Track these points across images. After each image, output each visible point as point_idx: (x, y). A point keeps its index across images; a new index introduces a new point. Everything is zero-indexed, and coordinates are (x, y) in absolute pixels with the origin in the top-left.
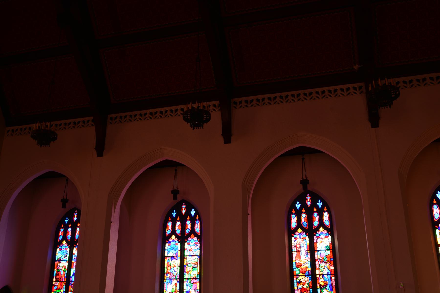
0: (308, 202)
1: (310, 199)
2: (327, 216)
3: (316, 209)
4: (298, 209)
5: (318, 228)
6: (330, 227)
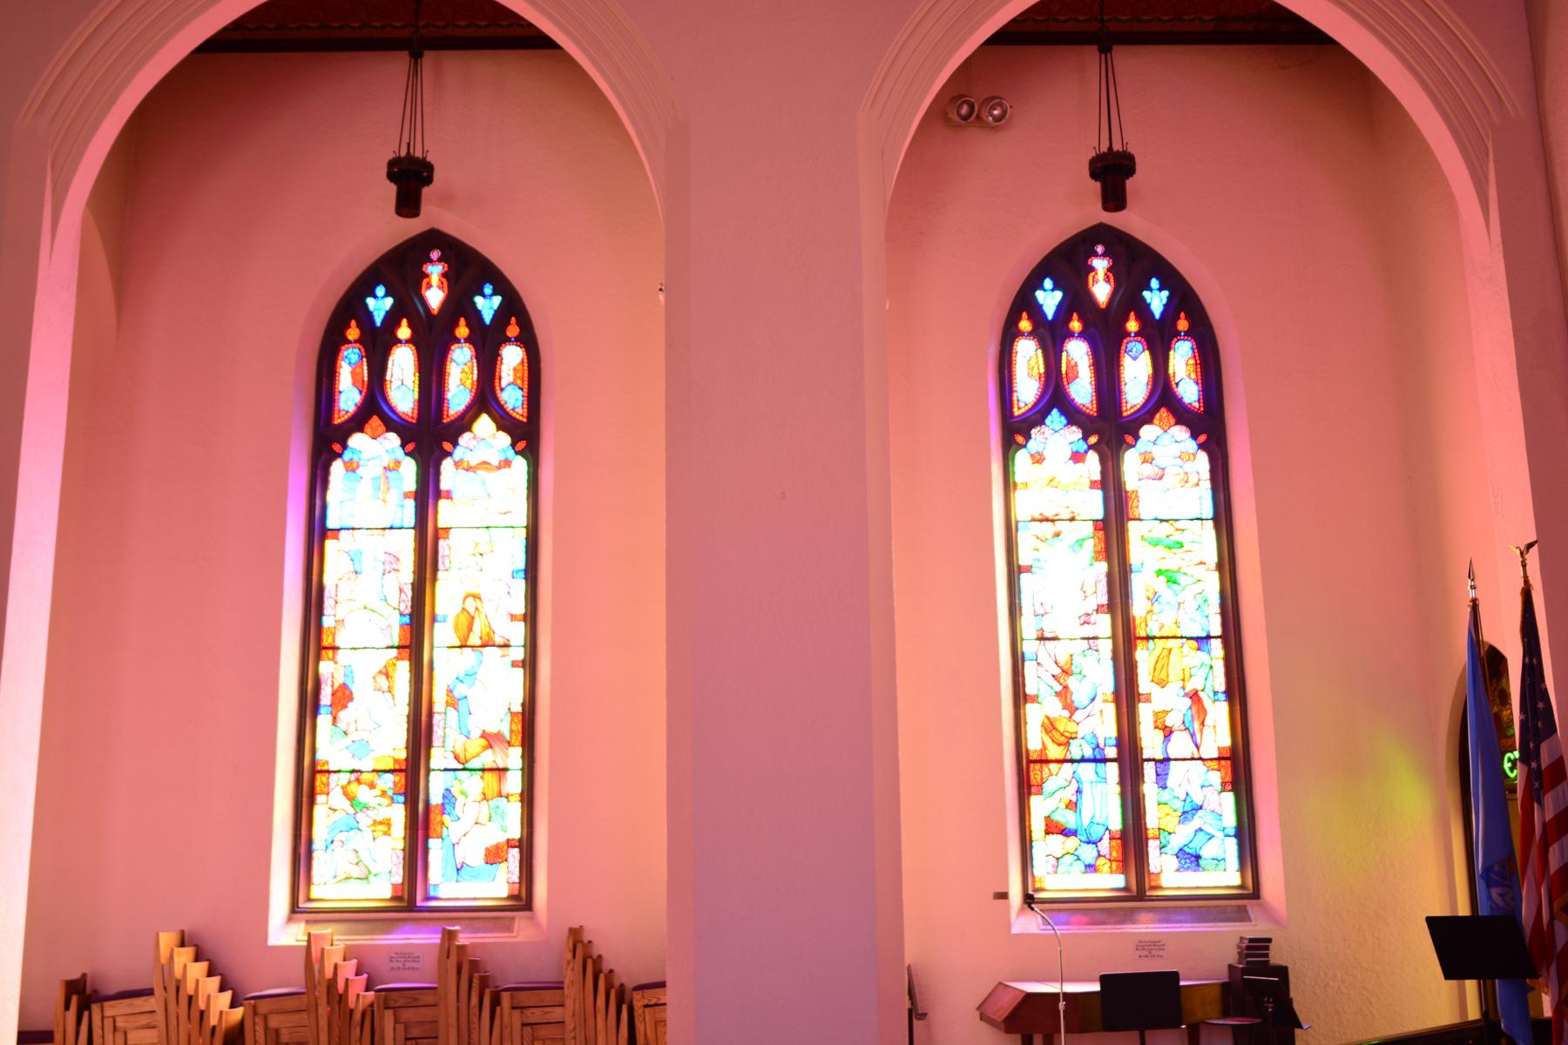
4: (378, 323)
5: (464, 423)
6: (528, 418)
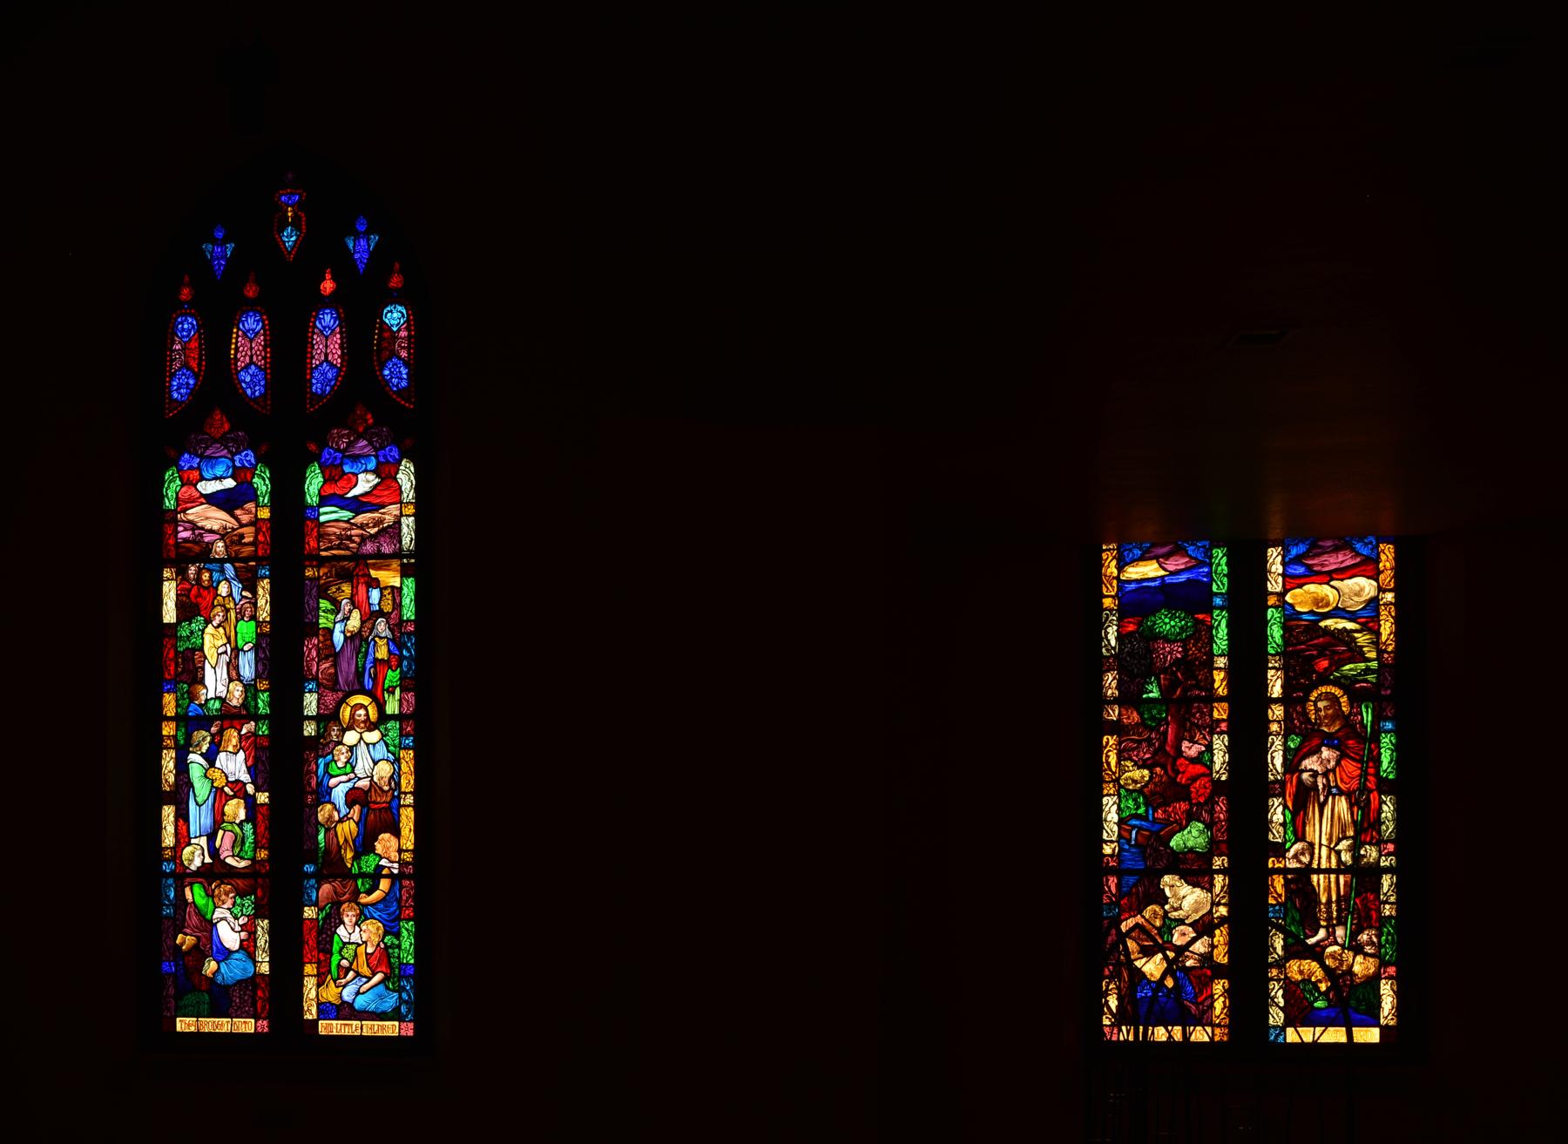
1: (298, 206)
3: (334, 278)
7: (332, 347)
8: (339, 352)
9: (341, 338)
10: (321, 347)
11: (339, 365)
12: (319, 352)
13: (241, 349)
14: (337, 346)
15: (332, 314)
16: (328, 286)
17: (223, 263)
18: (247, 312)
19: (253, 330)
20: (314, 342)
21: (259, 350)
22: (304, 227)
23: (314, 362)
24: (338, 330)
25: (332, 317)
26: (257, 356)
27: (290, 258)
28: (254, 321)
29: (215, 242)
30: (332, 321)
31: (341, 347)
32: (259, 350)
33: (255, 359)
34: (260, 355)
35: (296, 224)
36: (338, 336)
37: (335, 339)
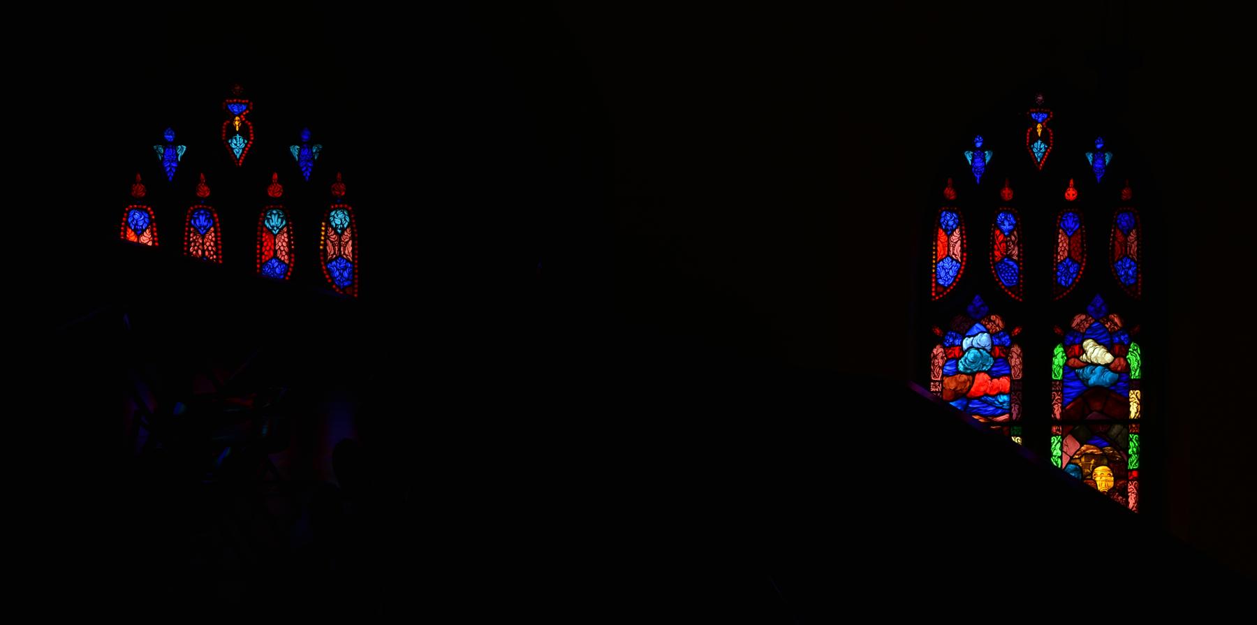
0: (232, 133)
2: (347, 234)
7: (280, 244)
8: (286, 249)
9: (289, 237)
10: (269, 244)
11: (287, 262)
12: (268, 248)
13: (193, 244)
14: (284, 244)
15: (279, 215)
16: (275, 191)
17: (174, 165)
18: (199, 210)
19: (205, 227)
20: (264, 240)
21: (210, 245)
22: (252, 135)
23: (263, 257)
24: (285, 229)
25: (278, 218)
26: (209, 251)
27: (238, 163)
28: (206, 219)
29: (166, 144)
30: (280, 220)
31: (289, 244)
32: (210, 245)
33: (207, 253)
34: (212, 250)
35: (244, 132)
36: (285, 235)
37: (283, 238)
